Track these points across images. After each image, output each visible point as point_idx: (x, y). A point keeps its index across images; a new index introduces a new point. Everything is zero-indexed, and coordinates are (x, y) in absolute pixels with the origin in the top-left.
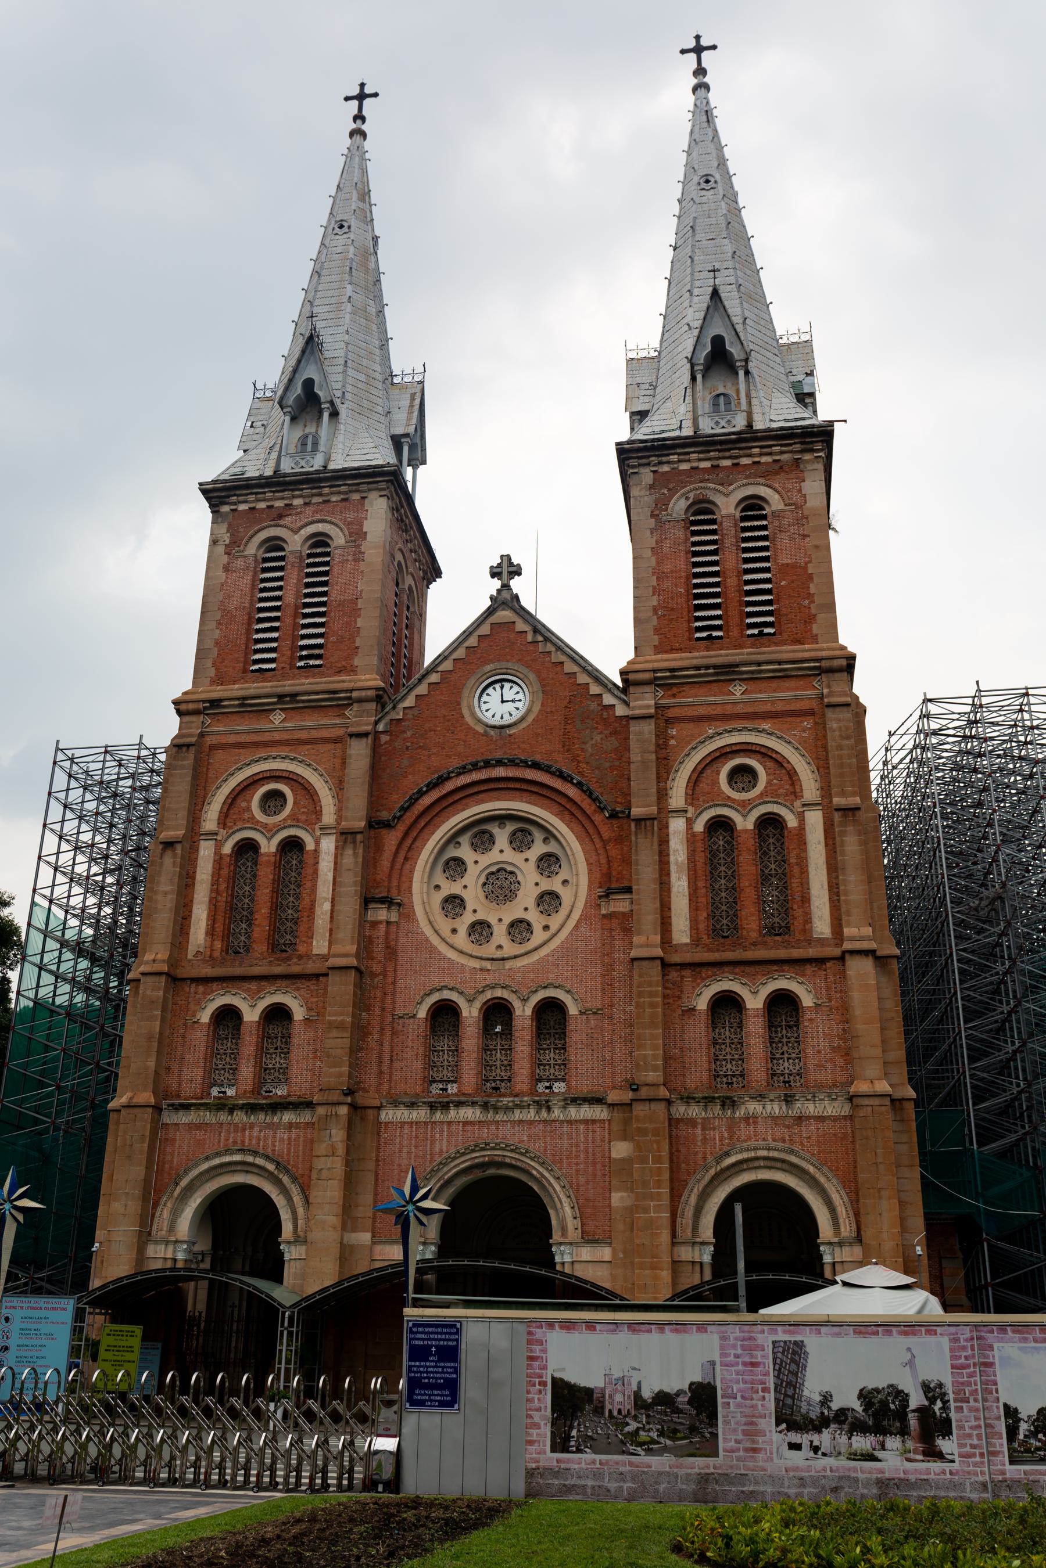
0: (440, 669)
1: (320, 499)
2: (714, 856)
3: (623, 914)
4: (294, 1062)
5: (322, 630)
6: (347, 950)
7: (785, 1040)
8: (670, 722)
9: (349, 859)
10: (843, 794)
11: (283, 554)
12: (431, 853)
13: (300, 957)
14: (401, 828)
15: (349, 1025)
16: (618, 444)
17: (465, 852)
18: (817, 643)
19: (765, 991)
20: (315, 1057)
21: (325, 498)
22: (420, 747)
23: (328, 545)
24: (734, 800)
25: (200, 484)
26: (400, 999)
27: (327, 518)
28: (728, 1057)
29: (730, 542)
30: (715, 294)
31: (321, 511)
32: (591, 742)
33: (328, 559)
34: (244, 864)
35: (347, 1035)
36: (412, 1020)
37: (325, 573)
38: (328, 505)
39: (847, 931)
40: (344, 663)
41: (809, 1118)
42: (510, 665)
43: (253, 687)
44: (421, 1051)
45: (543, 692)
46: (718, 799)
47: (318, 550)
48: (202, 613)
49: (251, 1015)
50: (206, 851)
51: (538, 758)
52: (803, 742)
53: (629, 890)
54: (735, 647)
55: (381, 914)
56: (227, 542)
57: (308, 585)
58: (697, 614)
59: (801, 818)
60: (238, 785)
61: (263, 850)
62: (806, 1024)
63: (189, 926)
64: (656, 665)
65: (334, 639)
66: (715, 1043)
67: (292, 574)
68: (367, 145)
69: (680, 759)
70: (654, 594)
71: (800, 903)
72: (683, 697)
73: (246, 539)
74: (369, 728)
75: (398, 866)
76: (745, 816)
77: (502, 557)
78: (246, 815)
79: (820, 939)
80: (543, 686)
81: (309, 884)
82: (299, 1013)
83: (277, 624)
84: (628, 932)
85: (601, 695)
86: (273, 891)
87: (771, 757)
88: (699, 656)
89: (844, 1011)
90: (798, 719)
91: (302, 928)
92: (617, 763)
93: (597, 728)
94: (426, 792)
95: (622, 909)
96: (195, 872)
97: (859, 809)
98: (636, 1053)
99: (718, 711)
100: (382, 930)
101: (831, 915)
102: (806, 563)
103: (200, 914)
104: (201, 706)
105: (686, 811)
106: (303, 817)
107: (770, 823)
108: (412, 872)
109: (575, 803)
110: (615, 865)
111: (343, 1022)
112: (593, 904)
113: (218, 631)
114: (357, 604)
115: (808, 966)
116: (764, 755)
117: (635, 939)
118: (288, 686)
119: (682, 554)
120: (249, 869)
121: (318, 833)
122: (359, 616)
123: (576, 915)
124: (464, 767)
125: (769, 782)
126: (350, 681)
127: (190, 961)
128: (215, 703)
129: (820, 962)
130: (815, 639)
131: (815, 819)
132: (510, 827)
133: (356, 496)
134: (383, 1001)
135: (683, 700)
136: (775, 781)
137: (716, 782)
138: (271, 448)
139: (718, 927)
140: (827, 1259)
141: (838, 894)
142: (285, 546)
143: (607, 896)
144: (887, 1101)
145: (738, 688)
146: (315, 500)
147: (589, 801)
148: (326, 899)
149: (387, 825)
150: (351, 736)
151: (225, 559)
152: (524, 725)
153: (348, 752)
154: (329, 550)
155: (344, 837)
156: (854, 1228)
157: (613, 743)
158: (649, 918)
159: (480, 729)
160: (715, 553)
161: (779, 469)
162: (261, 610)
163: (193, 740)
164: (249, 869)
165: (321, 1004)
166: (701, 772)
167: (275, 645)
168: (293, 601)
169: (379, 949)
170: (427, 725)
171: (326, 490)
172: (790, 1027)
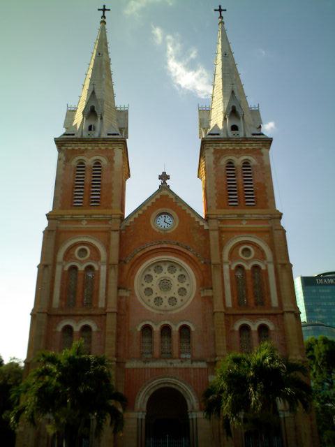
6: (112, 306)
9: (114, 274)
17: (152, 273)
29: (240, 174)
30: (233, 92)
37: (100, 173)
46: (238, 258)
49: (77, 328)
50: (59, 269)
51: (178, 242)
53: (212, 288)
55: (124, 293)
57: (94, 177)
59: (266, 266)
66: (241, 341)
68: (107, 26)
74: (118, 228)
82: (94, 328)
85: (198, 222)
107: (256, 267)
112: (198, 293)
117: (215, 306)
121: (100, 264)
125: (255, 255)
128: (62, 215)
129: (275, 315)
131: (271, 268)
132: (168, 265)
133: (110, 148)
137: (238, 253)
140: (281, 416)
146: (96, 148)
152: (172, 230)
157: (203, 238)
159: (158, 231)
162: (77, 184)
163: (55, 229)
167: (81, 197)
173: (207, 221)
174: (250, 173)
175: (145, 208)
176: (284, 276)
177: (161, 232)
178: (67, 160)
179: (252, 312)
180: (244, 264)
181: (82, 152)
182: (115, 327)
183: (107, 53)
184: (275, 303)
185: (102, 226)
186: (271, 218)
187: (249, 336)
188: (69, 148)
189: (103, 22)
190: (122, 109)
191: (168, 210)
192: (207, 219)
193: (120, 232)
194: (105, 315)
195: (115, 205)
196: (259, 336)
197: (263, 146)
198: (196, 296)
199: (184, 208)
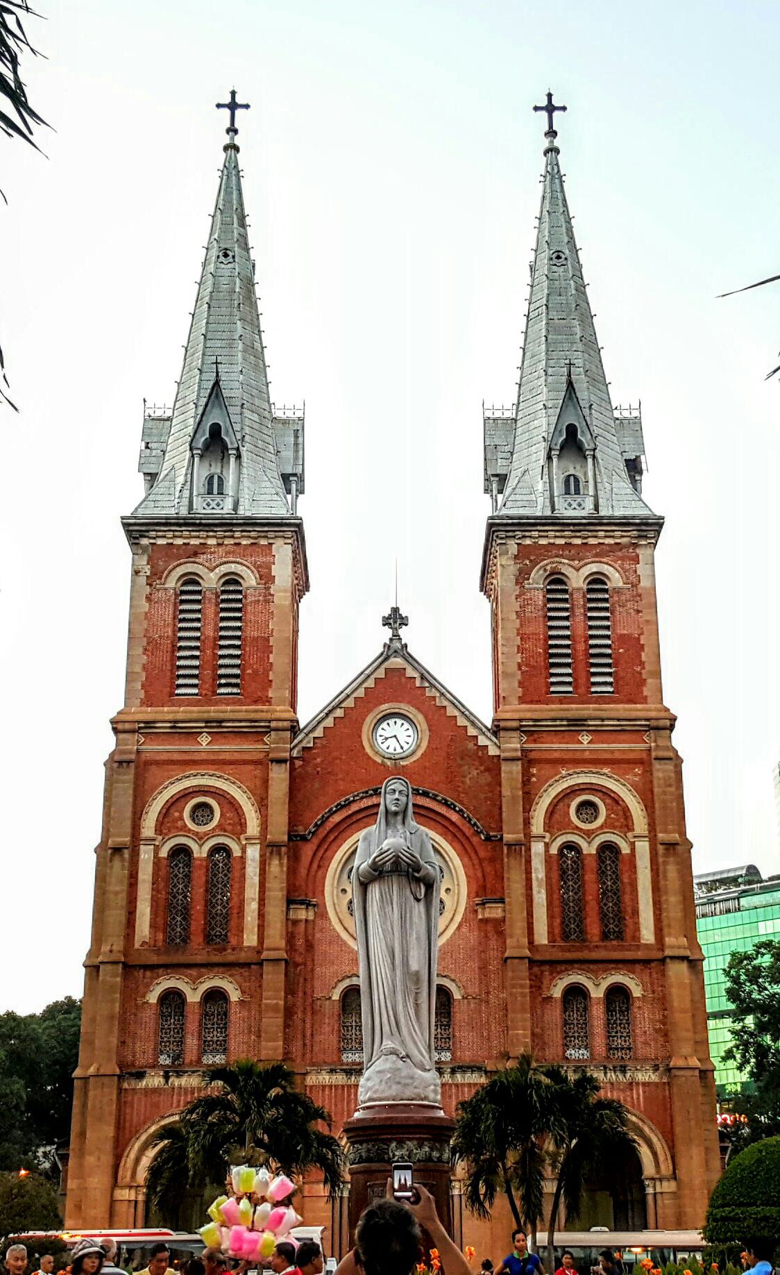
0: (342, 705)
1: (232, 541)
2: (564, 872)
4: (232, 1036)
5: (238, 662)
7: (618, 1022)
10: (666, 831)
11: (200, 588)
12: (340, 862)
14: (316, 841)
15: (282, 1008)
18: (646, 703)
19: (605, 985)
20: (250, 1032)
21: (237, 541)
22: (329, 773)
23: (238, 583)
24: (580, 830)
25: (123, 518)
26: (317, 984)
27: (238, 560)
28: (576, 1034)
29: (579, 611)
32: (469, 776)
34: (176, 865)
35: (281, 1014)
36: (328, 1002)
37: (239, 610)
38: (239, 547)
39: (668, 940)
40: (259, 694)
41: (638, 1084)
42: (402, 705)
43: (182, 712)
44: (336, 1027)
45: (430, 730)
46: (567, 826)
48: (131, 639)
50: (146, 854)
52: (635, 786)
53: (502, 901)
54: (583, 703)
55: (302, 914)
56: (148, 574)
57: (223, 619)
58: (553, 671)
60: (172, 797)
61: (195, 855)
62: (636, 1010)
63: (135, 920)
64: (522, 715)
65: (249, 671)
66: (565, 1023)
67: (210, 611)
71: (631, 915)
73: (166, 572)
75: (313, 872)
77: (392, 608)
79: (646, 945)
80: (430, 726)
81: (236, 886)
82: (234, 996)
83: (197, 653)
84: (501, 934)
85: (477, 737)
86: (206, 891)
87: (610, 796)
88: (553, 709)
89: (662, 1001)
90: (631, 766)
91: (233, 923)
92: (489, 795)
93: (474, 765)
94: (335, 812)
96: (137, 873)
98: (510, 1032)
99: (570, 756)
100: (302, 926)
101: (655, 925)
102: (639, 635)
104: (136, 726)
105: (544, 837)
107: (608, 849)
108: (324, 878)
109: (457, 826)
110: (490, 879)
111: (277, 1004)
112: (472, 910)
114: (268, 641)
115: (637, 965)
117: (508, 942)
118: (213, 711)
119: (541, 619)
120: (181, 870)
122: (271, 652)
123: (458, 918)
124: (367, 792)
125: (608, 816)
126: (267, 712)
128: (149, 724)
129: (646, 962)
130: (644, 700)
133: (263, 542)
134: (305, 987)
136: (613, 816)
139: (567, 930)
140: (650, 1190)
141: (660, 909)
143: (483, 904)
144: (697, 1073)
145: (585, 737)
148: (253, 899)
149: (304, 839)
150: (272, 761)
151: (148, 589)
152: (415, 758)
154: (241, 589)
155: (270, 848)
156: (671, 1168)
157: (486, 778)
159: (379, 760)
160: (567, 618)
163: (133, 757)
164: (181, 870)
165: (253, 988)
167: (196, 672)
168: (212, 634)
169: (300, 942)
170: (336, 754)
171: (237, 534)
172: (623, 1012)
173: (495, 734)
174: (606, 609)
175: (350, 703)
176: (672, 871)
177: (389, 763)
178: (156, 576)
179: (595, 955)
180: (583, 844)
183: (246, 248)
184: (647, 935)
185: (249, 748)
187: (585, 1009)
188: (160, 542)
189: (232, 148)
190: (289, 414)
191: (405, 708)
192: (497, 729)
193: (292, 764)
194: (260, 964)
196: (609, 1010)
197: (640, 537)
199: (441, 702)
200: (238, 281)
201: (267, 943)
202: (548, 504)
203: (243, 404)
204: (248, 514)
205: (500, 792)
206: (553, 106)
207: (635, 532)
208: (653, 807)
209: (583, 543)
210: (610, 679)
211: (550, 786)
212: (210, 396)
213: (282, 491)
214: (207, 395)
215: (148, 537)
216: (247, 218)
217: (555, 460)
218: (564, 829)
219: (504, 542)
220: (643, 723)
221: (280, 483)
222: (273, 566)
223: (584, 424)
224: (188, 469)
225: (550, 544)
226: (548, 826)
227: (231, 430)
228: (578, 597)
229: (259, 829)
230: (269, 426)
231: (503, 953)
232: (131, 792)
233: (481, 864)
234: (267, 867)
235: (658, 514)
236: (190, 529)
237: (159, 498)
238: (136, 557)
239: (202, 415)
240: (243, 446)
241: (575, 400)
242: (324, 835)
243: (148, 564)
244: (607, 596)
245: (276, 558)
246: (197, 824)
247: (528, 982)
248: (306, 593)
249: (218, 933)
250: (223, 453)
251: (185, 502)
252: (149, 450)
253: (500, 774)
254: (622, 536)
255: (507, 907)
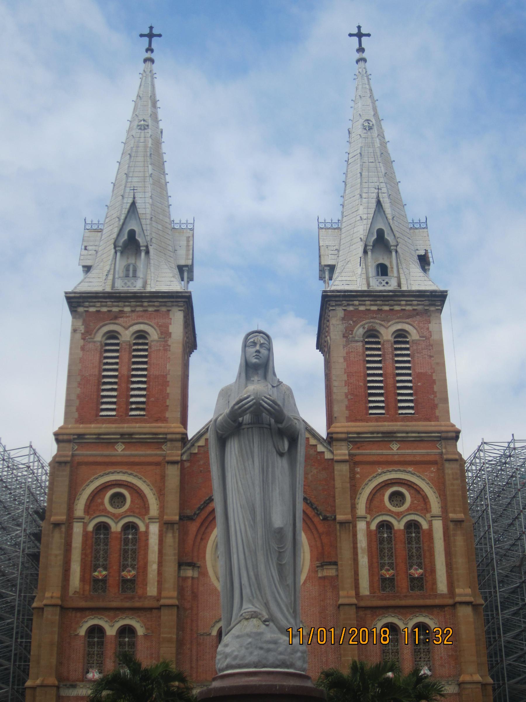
1: (141, 309)
3: (332, 577)
5: (144, 393)
8: (357, 464)
9: (170, 539)
10: (455, 512)
13: (140, 598)
14: (199, 521)
16: (324, 291)
18: (438, 421)
21: (145, 309)
23: (145, 338)
24: (392, 512)
25: (66, 293)
27: (146, 321)
29: (389, 357)
31: (142, 316)
32: (312, 474)
33: (146, 347)
36: (208, 637)
47: (141, 341)
49: (111, 631)
50: (78, 529)
53: (335, 564)
54: (392, 421)
55: (189, 573)
56: (83, 331)
58: (371, 399)
59: (430, 523)
60: (96, 488)
63: (69, 576)
65: (153, 399)
67: (125, 356)
69: (362, 487)
70: (345, 386)
72: (364, 450)
73: (95, 331)
74: (179, 458)
76: (399, 521)
78: (101, 507)
82: (140, 631)
83: (115, 387)
85: (316, 445)
87: (413, 487)
95: (331, 574)
96: (71, 542)
97: (463, 521)
98: (343, 659)
99: (384, 459)
100: (190, 582)
102: (432, 373)
103: (76, 568)
104: (72, 437)
106: (137, 511)
107: (412, 526)
108: (205, 547)
112: (313, 570)
113: (79, 389)
114: (166, 378)
116: (409, 486)
117: (341, 593)
118: (126, 428)
121: (147, 521)
122: (168, 386)
125: (412, 502)
126: (165, 428)
127: (71, 597)
128: (80, 436)
129: (441, 607)
130: (437, 419)
131: (438, 526)
133: (164, 309)
135: (364, 451)
136: (415, 502)
137: (382, 501)
138: (109, 271)
142: (119, 336)
143: (322, 566)
145: (395, 446)
146: (138, 309)
147: (310, 509)
149: (191, 518)
150: (169, 462)
151: (82, 342)
153: (167, 472)
154: (147, 341)
158: (348, 582)
160: (379, 362)
161: (415, 313)
163: (69, 459)
166: (374, 495)
167: (114, 400)
171: (146, 304)
179: (403, 603)
181: (115, 317)
182: (175, 630)
184: (442, 586)
186: (441, 439)
188: (92, 309)
190: (184, 226)
192: (331, 440)
195: (173, 414)
198: (308, 578)
200: (150, 140)
201: (164, 594)
202: (365, 282)
203: (152, 218)
204: (153, 290)
205: (334, 485)
206: (362, 33)
207: (427, 302)
208: (445, 495)
209: (391, 310)
210: (411, 405)
211: (370, 480)
212: (129, 212)
213: (178, 276)
214: (126, 212)
215: (83, 306)
216: (158, 103)
217: (369, 253)
218: (381, 512)
219: (334, 308)
220: (437, 435)
221: (176, 271)
222: (170, 326)
223: (389, 228)
224: (112, 261)
225: (366, 310)
226: (369, 509)
227: (142, 233)
228: (388, 346)
229: (158, 512)
230: (170, 233)
231: (337, 601)
232: (67, 483)
233: (320, 537)
234: (164, 538)
235: (442, 288)
236: (113, 300)
237: (91, 280)
238: (74, 319)
239: (124, 224)
240: (151, 245)
241: (383, 213)
242: (206, 516)
243: (83, 325)
244: (408, 346)
245: (172, 321)
246: (114, 508)
247: (356, 622)
248: (195, 351)
249: (129, 587)
250: (137, 250)
251: (109, 282)
252: (86, 251)
253: (334, 472)
254: (418, 305)
255: (340, 568)
